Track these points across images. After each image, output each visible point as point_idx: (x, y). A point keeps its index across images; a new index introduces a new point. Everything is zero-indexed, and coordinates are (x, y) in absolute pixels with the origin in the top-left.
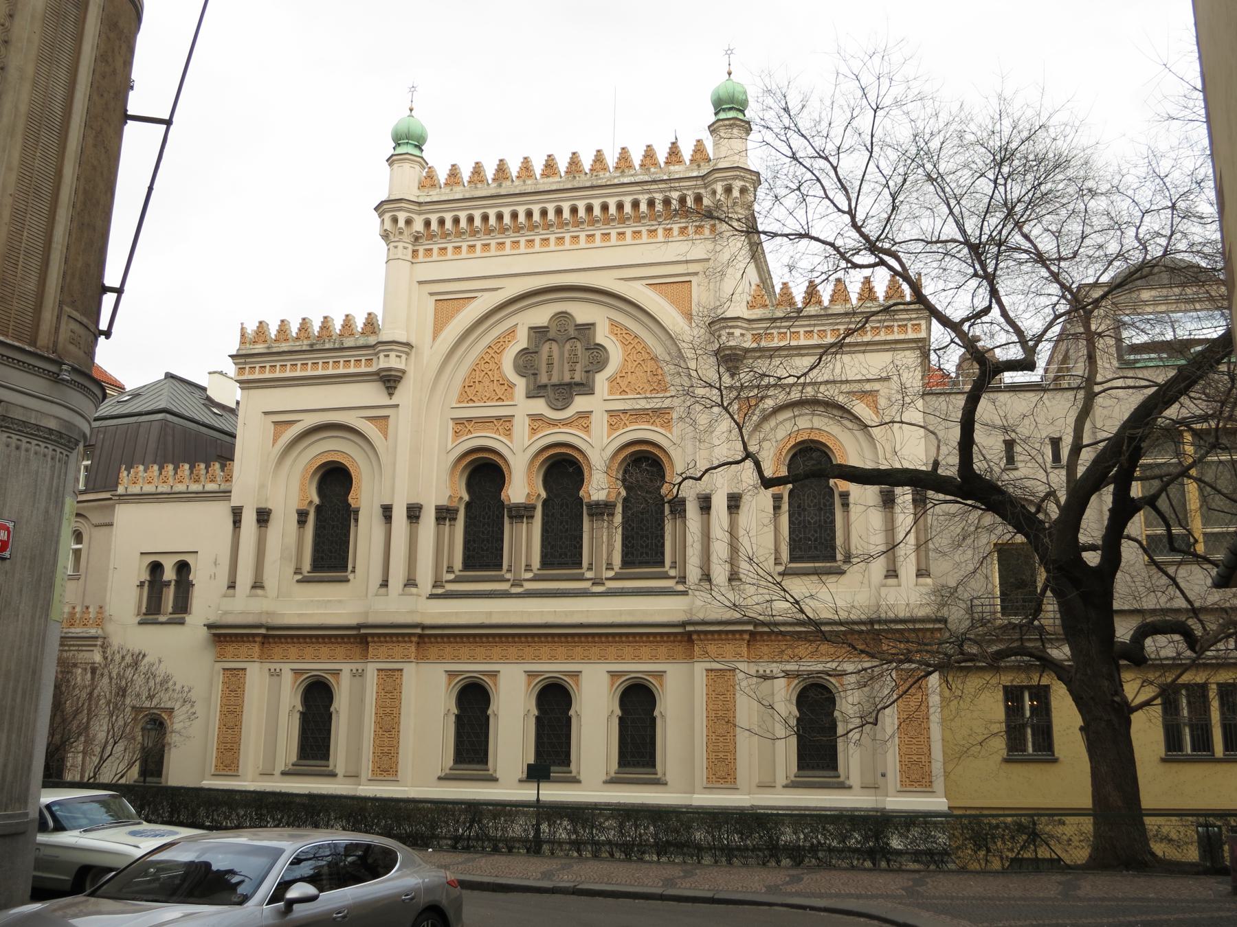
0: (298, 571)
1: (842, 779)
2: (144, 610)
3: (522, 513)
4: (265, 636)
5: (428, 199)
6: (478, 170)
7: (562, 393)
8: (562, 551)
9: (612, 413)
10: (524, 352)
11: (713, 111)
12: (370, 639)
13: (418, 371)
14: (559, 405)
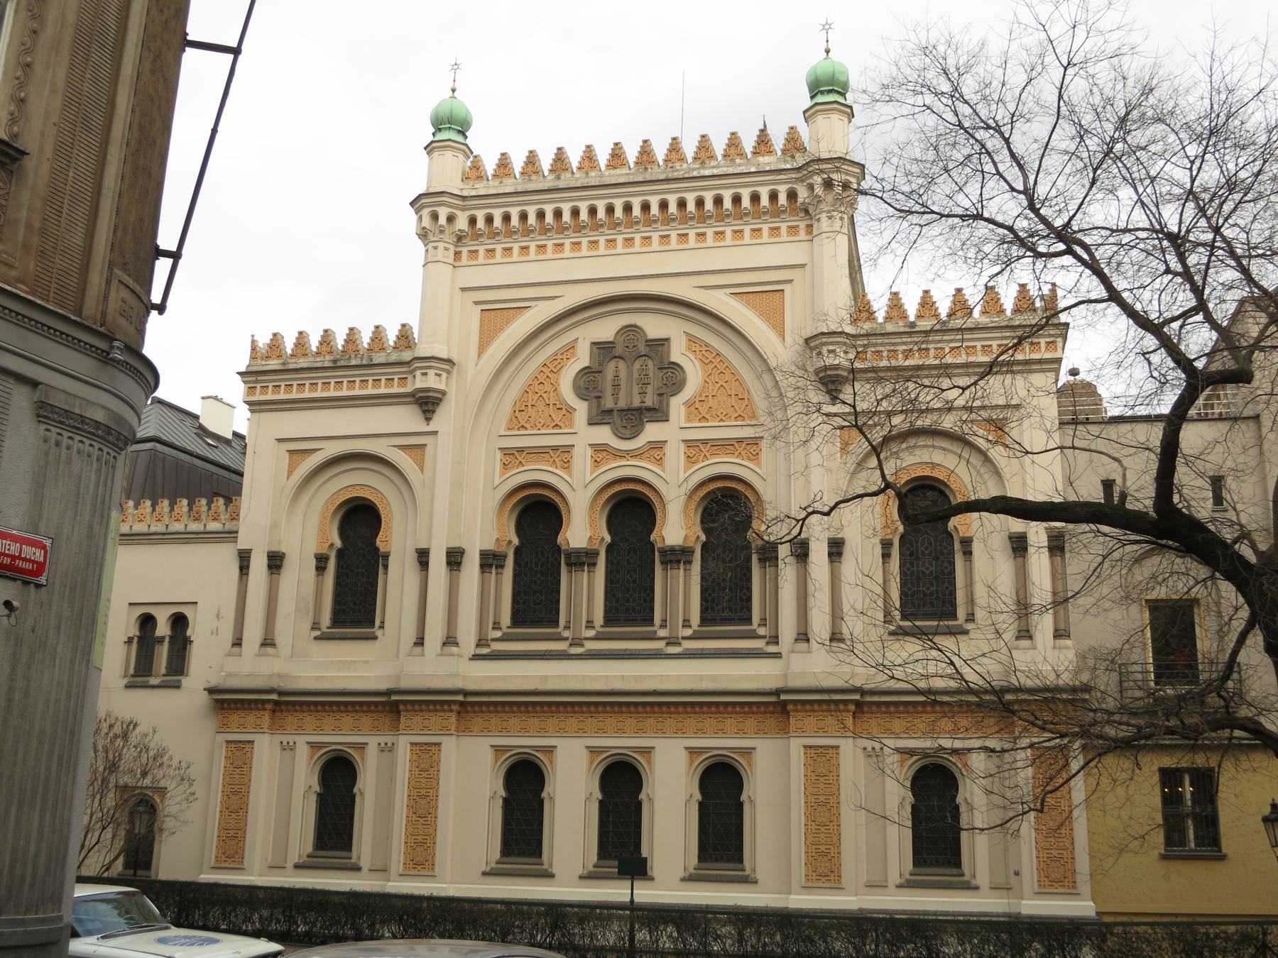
0: (315, 626)
1: (966, 878)
2: (132, 671)
3: (582, 559)
4: (276, 703)
5: (474, 193)
6: (532, 159)
7: (631, 419)
8: (630, 606)
9: (689, 443)
10: (585, 371)
11: (808, 96)
12: (401, 707)
13: (461, 393)
14: (627, 433)
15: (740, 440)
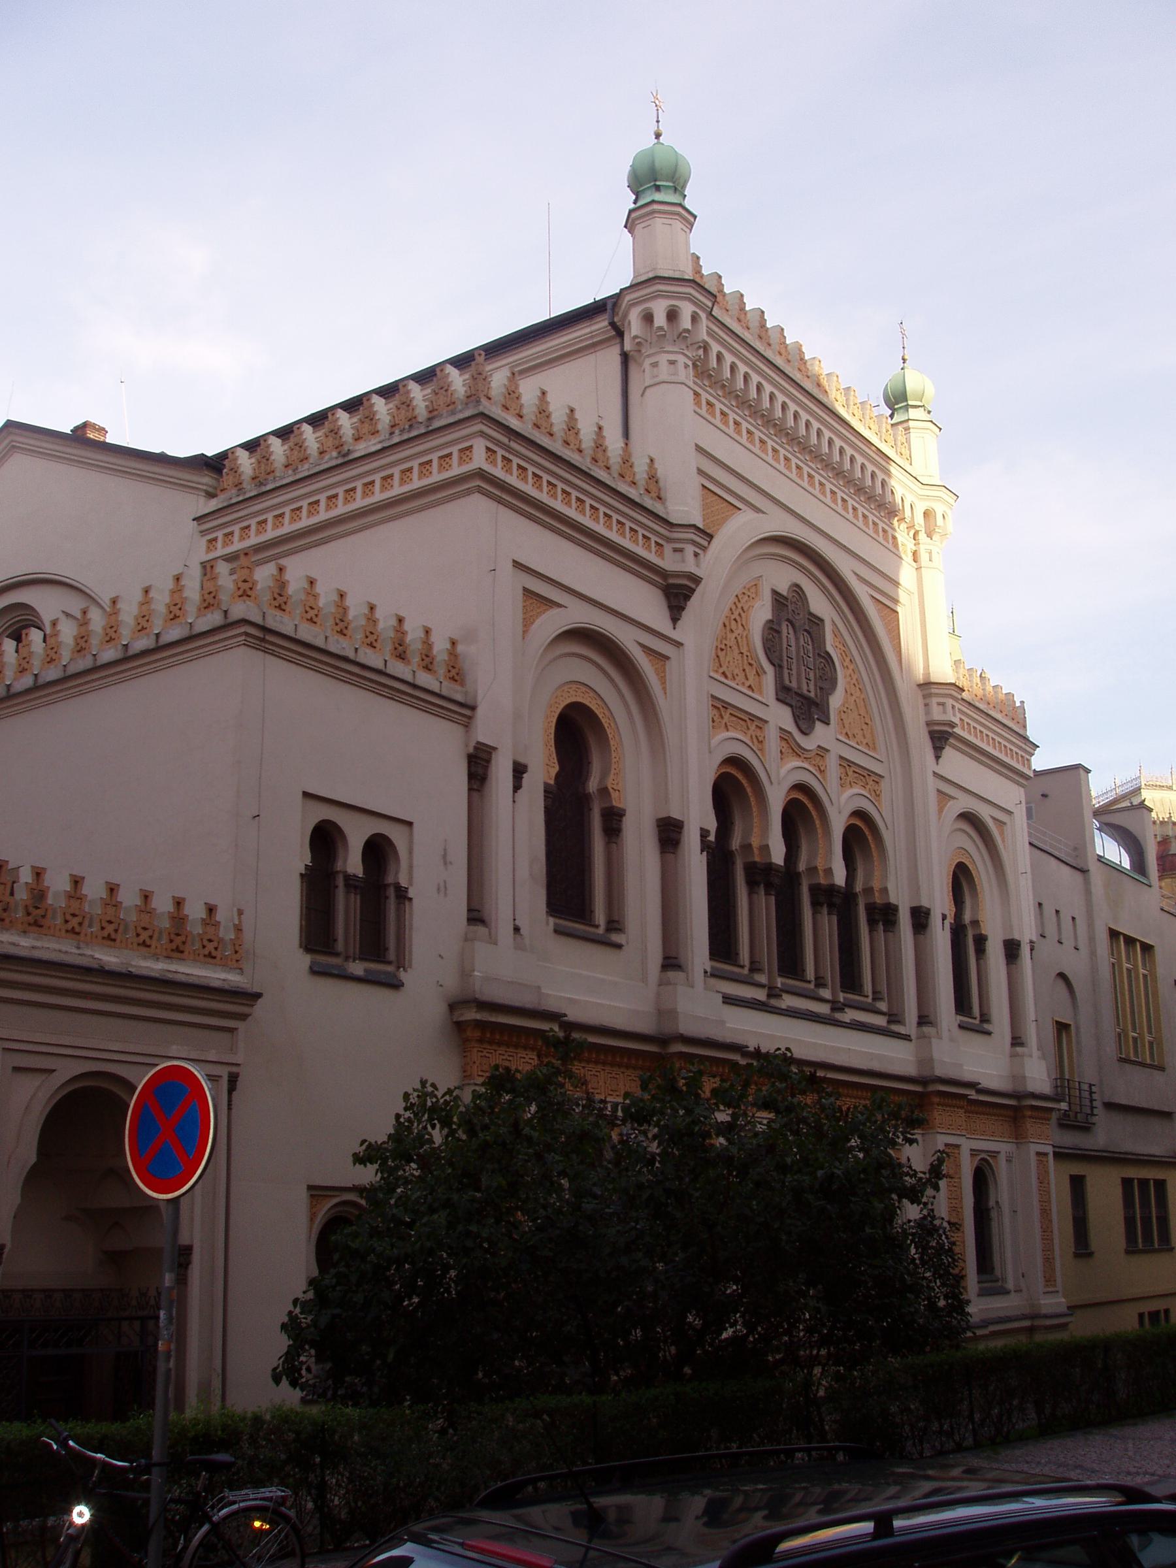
15: (871, 773)
